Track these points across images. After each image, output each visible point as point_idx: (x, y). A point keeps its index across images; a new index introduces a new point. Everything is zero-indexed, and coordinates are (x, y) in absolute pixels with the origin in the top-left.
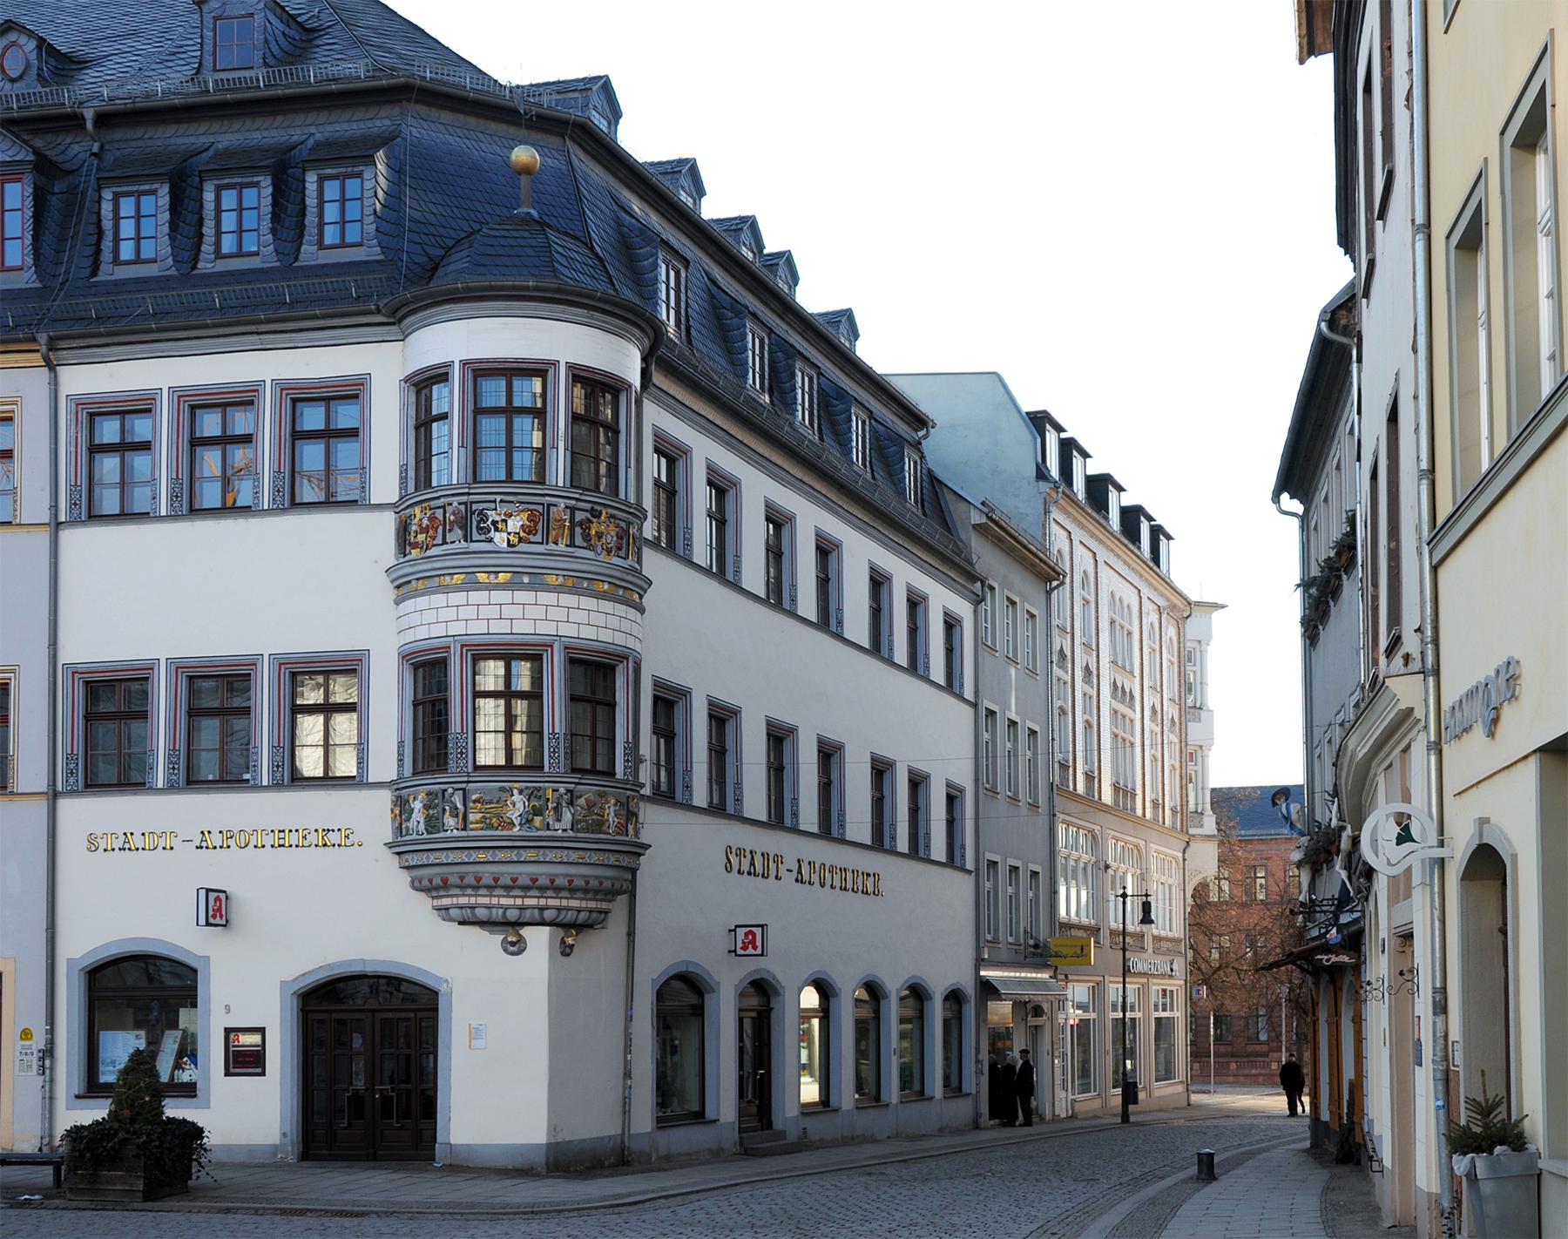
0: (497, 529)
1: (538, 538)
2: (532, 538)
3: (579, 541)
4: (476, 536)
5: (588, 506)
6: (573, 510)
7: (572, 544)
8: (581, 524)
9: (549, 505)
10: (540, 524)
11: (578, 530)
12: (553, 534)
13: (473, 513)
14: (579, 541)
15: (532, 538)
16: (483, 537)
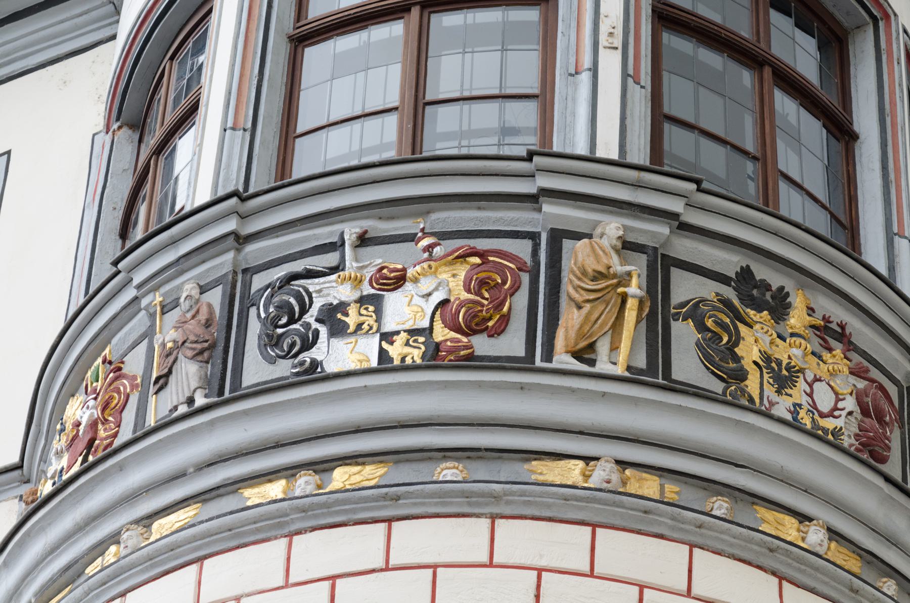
0: (338, 330)
1: (512, 343)
2: (482, 345)
3: (687, 364)
4: (256, 369)
5: (729, 261)
6: (661, 266)
7: (655, 372)
8: (695, 312)
9: (557, 237)
10: (511, 303)
11: (684, 334)
12: (571, 320)
13: (249, 302)
14: (687, 364)
15: (482, 345)
16: (284, 368)
